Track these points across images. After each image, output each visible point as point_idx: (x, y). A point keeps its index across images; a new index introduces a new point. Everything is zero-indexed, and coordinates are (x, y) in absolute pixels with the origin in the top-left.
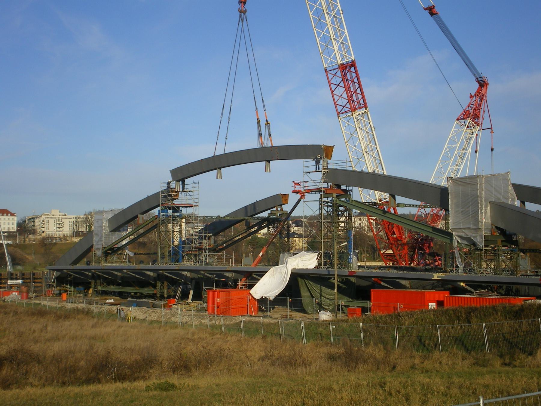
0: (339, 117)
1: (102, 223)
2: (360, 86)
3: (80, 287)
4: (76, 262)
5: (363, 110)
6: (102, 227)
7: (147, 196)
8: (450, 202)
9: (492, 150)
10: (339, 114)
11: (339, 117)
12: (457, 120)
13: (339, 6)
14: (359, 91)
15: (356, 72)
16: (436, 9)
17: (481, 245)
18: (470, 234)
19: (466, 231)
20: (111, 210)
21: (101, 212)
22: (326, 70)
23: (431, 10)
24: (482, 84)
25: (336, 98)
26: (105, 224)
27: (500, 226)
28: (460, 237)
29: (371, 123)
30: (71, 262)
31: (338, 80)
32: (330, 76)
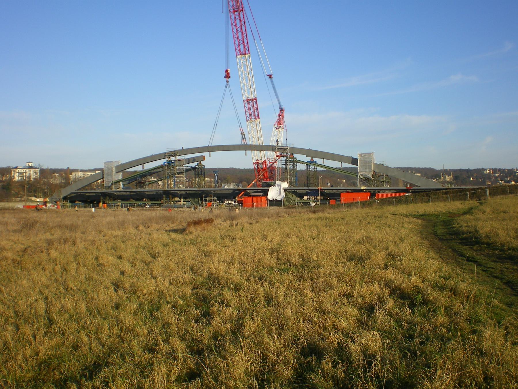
0: (247, 122)
1: (112, 168)
2: (257, 109)
3: (77, 202)
4: (78, 190)
5: (258, 120)
6: (112, 170)
7: (151, 155)
8: (359, 162)
9: (286, 139)
10: (247, 121)
11: (247, 122)
12: (275, 125)
13: (253, 73)
14: (256, 110)
15: (256, 102)
16: (272, 76)
17: (372, 178)
18: (366, 174)
19: (365, 173)
20: (116, 161)
21: (112, 162)
22: (244, 100)
23: (270, 77)
24: (282, 110)
25: (246, 112)
26: (114, 169)
27: (377, 171)
28: (361, 175)
29: (260, 126)
30: (77, 189)
31: (246, 105)
32: (245, 102)
